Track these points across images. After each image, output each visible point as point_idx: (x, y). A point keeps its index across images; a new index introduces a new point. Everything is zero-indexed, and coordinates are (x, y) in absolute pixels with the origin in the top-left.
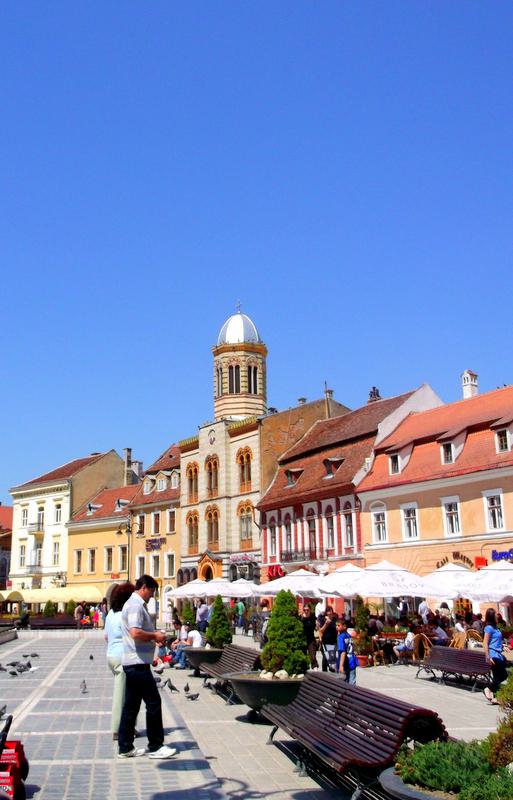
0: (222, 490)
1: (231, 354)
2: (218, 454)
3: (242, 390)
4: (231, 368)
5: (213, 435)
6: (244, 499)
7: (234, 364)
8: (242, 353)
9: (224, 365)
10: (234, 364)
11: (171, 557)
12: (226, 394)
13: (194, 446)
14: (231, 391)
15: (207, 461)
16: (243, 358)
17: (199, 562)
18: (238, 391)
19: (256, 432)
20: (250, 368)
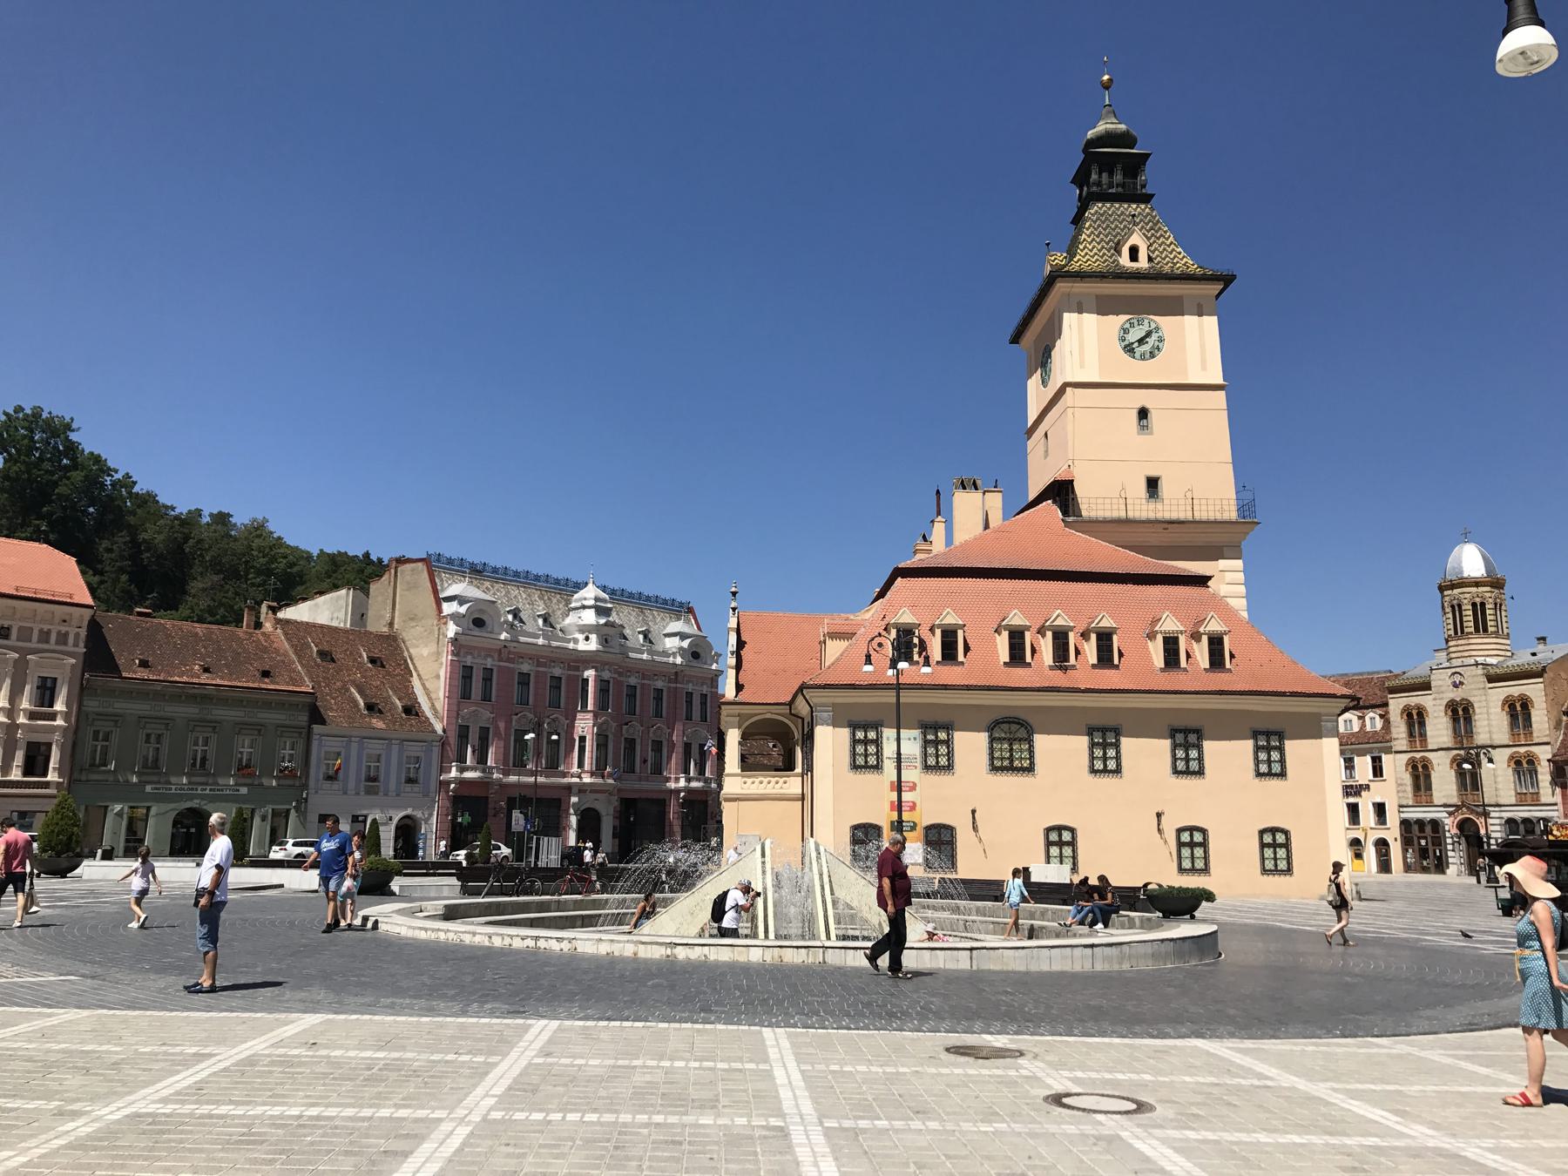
0: (1481, 737)
1: (1474, 589)
2: (1471, 699)
3: (1490, 629)
4: (1474, 605)
5: (1457, 679)
6: (1515, 749)
7: (1478, 600)
8: (1488, 589)
9: (1465, 601)
10: (1478, 600)
11: (1380, 809)
12: (1471, 633)
13: (1425, 686)
14: (1477, 630)
15: (1447, 706)
16: (1489, 595)
17: (1450, 814)
18: (1485, 630)
19: (1541, 680)
20: (1496, 604)
